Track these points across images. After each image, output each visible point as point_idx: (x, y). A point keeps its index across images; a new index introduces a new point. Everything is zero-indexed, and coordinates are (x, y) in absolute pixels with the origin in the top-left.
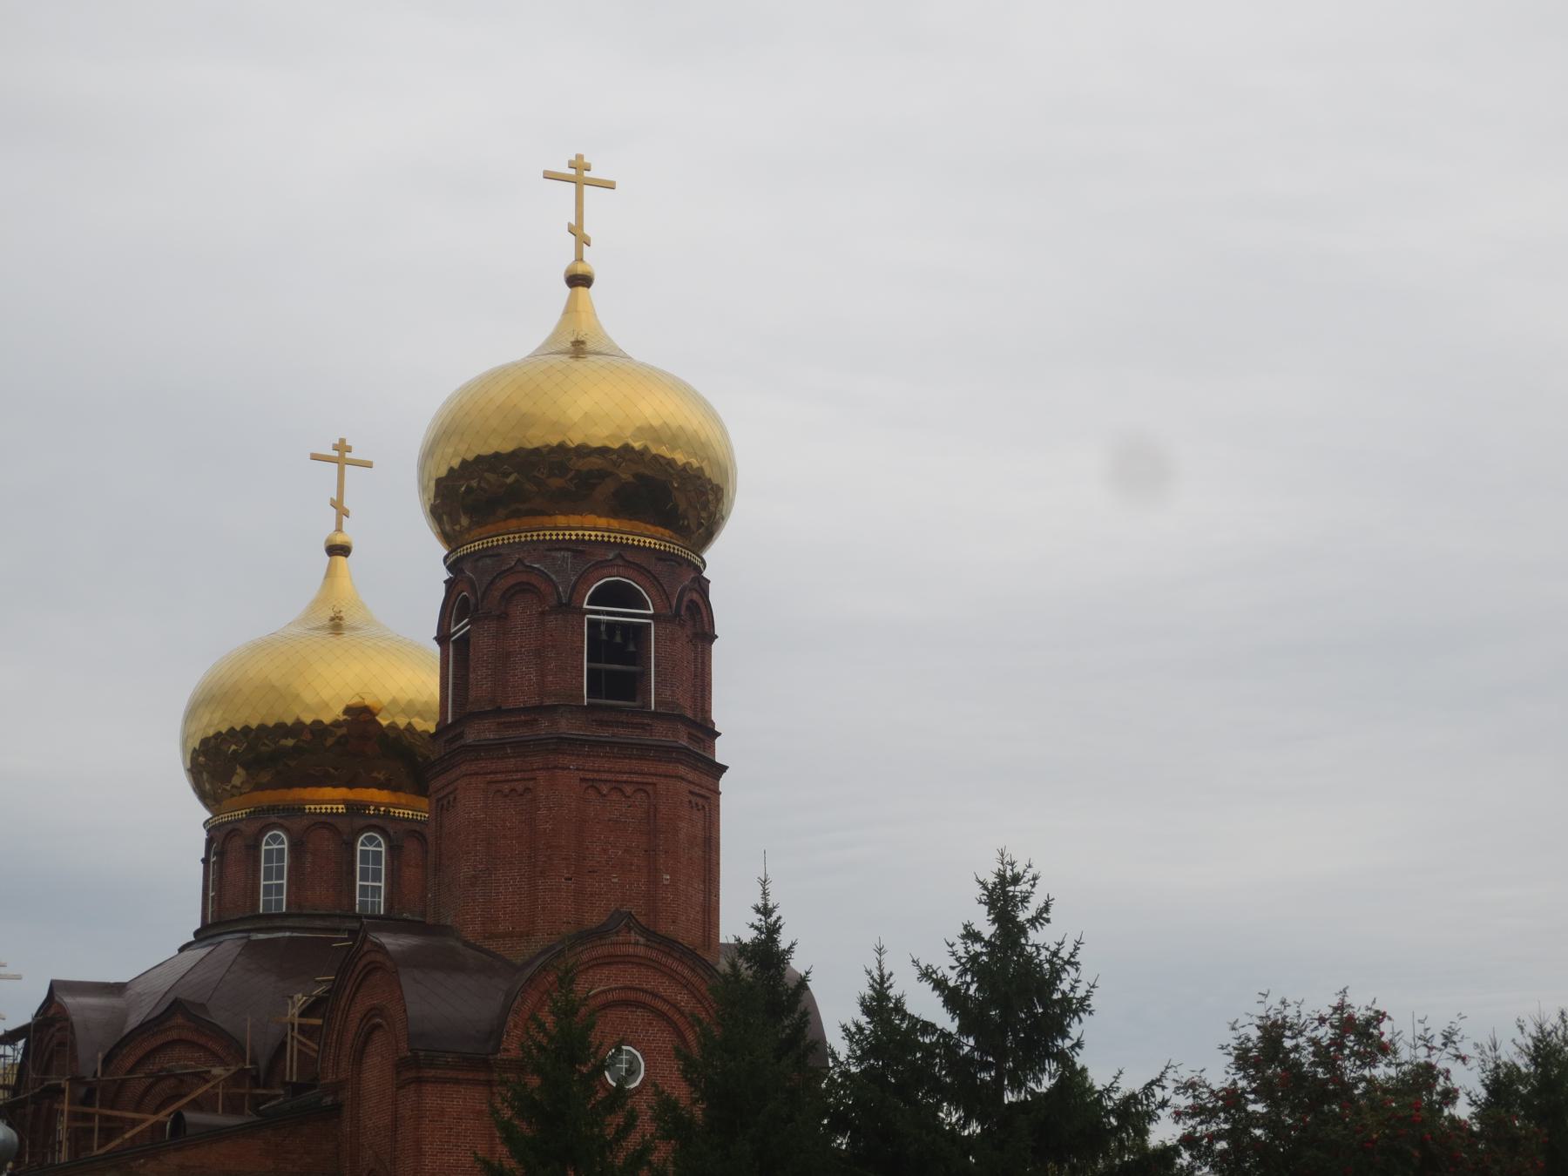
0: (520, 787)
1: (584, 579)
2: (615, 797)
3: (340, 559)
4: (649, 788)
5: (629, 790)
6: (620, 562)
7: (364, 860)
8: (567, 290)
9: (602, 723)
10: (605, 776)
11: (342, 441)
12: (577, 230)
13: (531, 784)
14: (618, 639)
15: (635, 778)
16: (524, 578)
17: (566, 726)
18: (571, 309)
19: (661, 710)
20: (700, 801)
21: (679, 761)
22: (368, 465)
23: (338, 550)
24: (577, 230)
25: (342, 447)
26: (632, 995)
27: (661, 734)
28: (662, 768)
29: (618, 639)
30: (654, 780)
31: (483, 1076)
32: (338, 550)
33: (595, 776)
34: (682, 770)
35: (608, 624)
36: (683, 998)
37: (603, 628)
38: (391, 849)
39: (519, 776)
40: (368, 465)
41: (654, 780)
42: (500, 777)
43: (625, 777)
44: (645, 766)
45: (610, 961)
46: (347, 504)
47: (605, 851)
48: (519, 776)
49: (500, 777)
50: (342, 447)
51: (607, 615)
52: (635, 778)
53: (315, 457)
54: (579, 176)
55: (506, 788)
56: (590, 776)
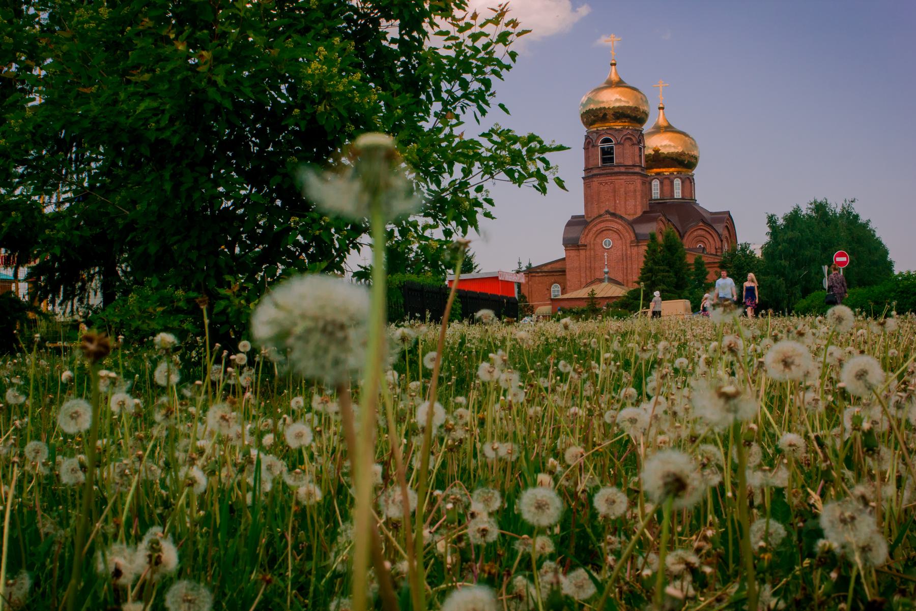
1: (598, 138)
17: (595, 172)
27: (616, 170)
36: (620, 227)
45: (603, 221)
51: (606, 145)
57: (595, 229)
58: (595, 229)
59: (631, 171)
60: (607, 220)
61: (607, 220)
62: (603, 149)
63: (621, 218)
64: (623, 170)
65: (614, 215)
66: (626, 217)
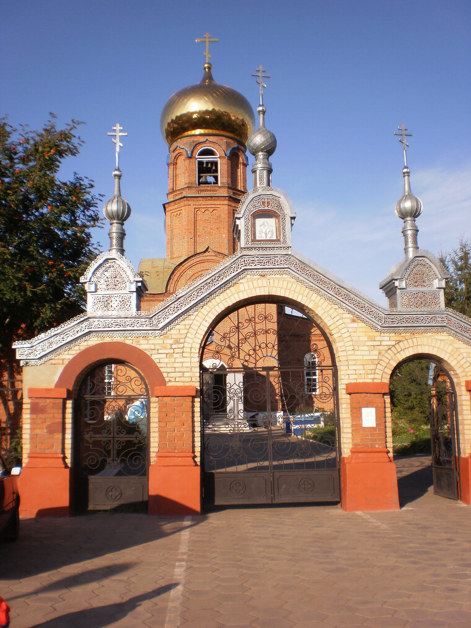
0: (178, 213)
10: (203, 206)
13: (181, 211)
14: (209, 166)
15: (213, 206)
16: (179, 151)
29: (209, 166)
35: (207, 163)
39: (178, 209)
41: (219, 206)
42: (174, 211)
44: (216, 202)
48: (178, 209)
49: (174, 211)
52: (213, 206)
55: (175, 214)
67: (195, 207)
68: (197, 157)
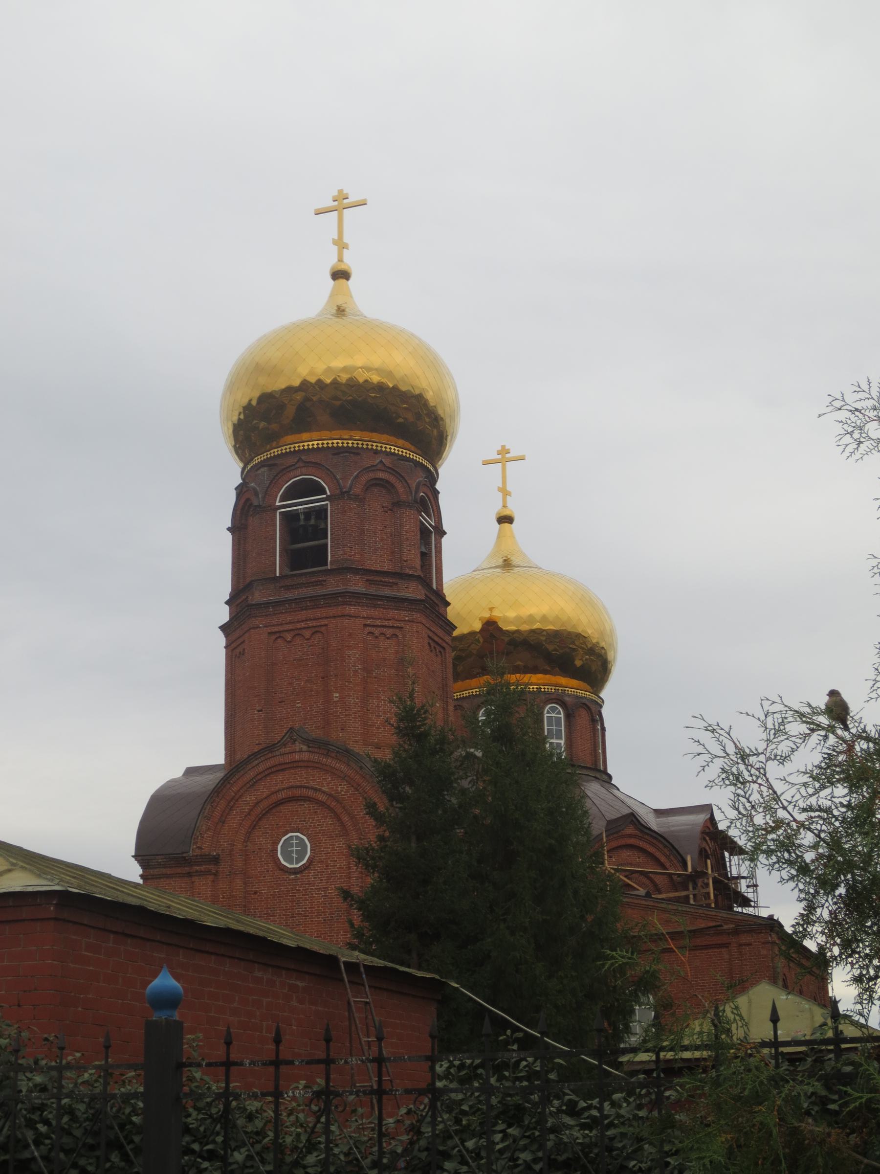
1: (274, 483)
2: (298, 641)
3: (506, 525)
4: (323, 629)
5: (307, 633)
6: (301, 464)
7: (550, 723)
8: (332, 282)
9: (288, 588)
10: (287, 627)
11: (503, 447)
12: (341, 245)
15: (311, 624)
18: (333, 295)
19: (334, 567)
20: (389, 632)
21: (345, 603)
22: (522, 458)
23: (505, 519)
24: (341, 245)
25: (504, 451)
26: (298, 792)
27: (334, 585)
28: (332, 611)
30: (325, 622)
31: (187, 869)
32: (505, 519)
33: (280, 628)
34: (351, 610)
36: (343, 789)
37: (302, 517)
38: (568, 716)
40: (522, 458)
41: (325, 622)
43: (303, 625)
44: (319, 613)
45: (281, 768)
46: (509, 488)
47: (291, 684)
50: (504, 451)
51: (301, 505)
52: (311, 624)
53: (485, 463)
54: (341, 204)
56: (276, 629)
57: (250, 798)
58: (250, 798)
59: (387, 592)
60: (295, 765)
61: (295, 765)
62: (290, 518)
63: (346, 754)
64: (358, 585)
65: (320, 745)
66: (358, 749)
67: (269, 630)
68: (278, 504)
